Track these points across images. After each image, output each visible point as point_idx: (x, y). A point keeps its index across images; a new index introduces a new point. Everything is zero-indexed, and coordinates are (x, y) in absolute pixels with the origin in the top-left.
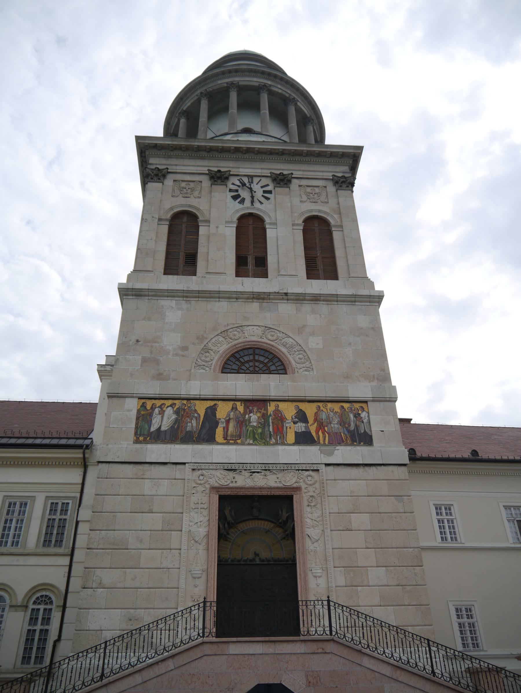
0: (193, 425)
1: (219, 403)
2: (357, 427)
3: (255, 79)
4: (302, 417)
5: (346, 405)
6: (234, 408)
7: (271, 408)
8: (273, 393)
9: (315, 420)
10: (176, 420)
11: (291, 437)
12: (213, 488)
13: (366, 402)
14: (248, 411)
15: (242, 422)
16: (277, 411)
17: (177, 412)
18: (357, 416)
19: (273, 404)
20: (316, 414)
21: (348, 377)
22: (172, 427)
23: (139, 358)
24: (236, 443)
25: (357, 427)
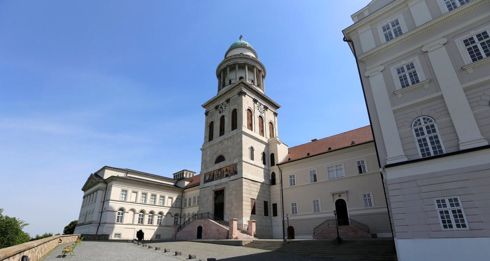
0: (211, 177)
1: (215, 171)
2: (236, 170)
3: (224, 65)
4: (227, 171)
5: (234, 165)
6: (217, 172)
7: (222, 170)
8: (222, 167)
9: (229, 170)
10: (209, 177)
11: (225, 176)
12: (213, 190)
13: (237, 163)
14: (219, 172)
15: (218, 175)
16: (223, 170)
17: (209, 175)
18: (236, 167)
19: (223, 169)
20: (229, 169)
21: (235, 158)
22: (208, 179)
23: (204, 165)
24: (217, 180)
25: (236, 170)
